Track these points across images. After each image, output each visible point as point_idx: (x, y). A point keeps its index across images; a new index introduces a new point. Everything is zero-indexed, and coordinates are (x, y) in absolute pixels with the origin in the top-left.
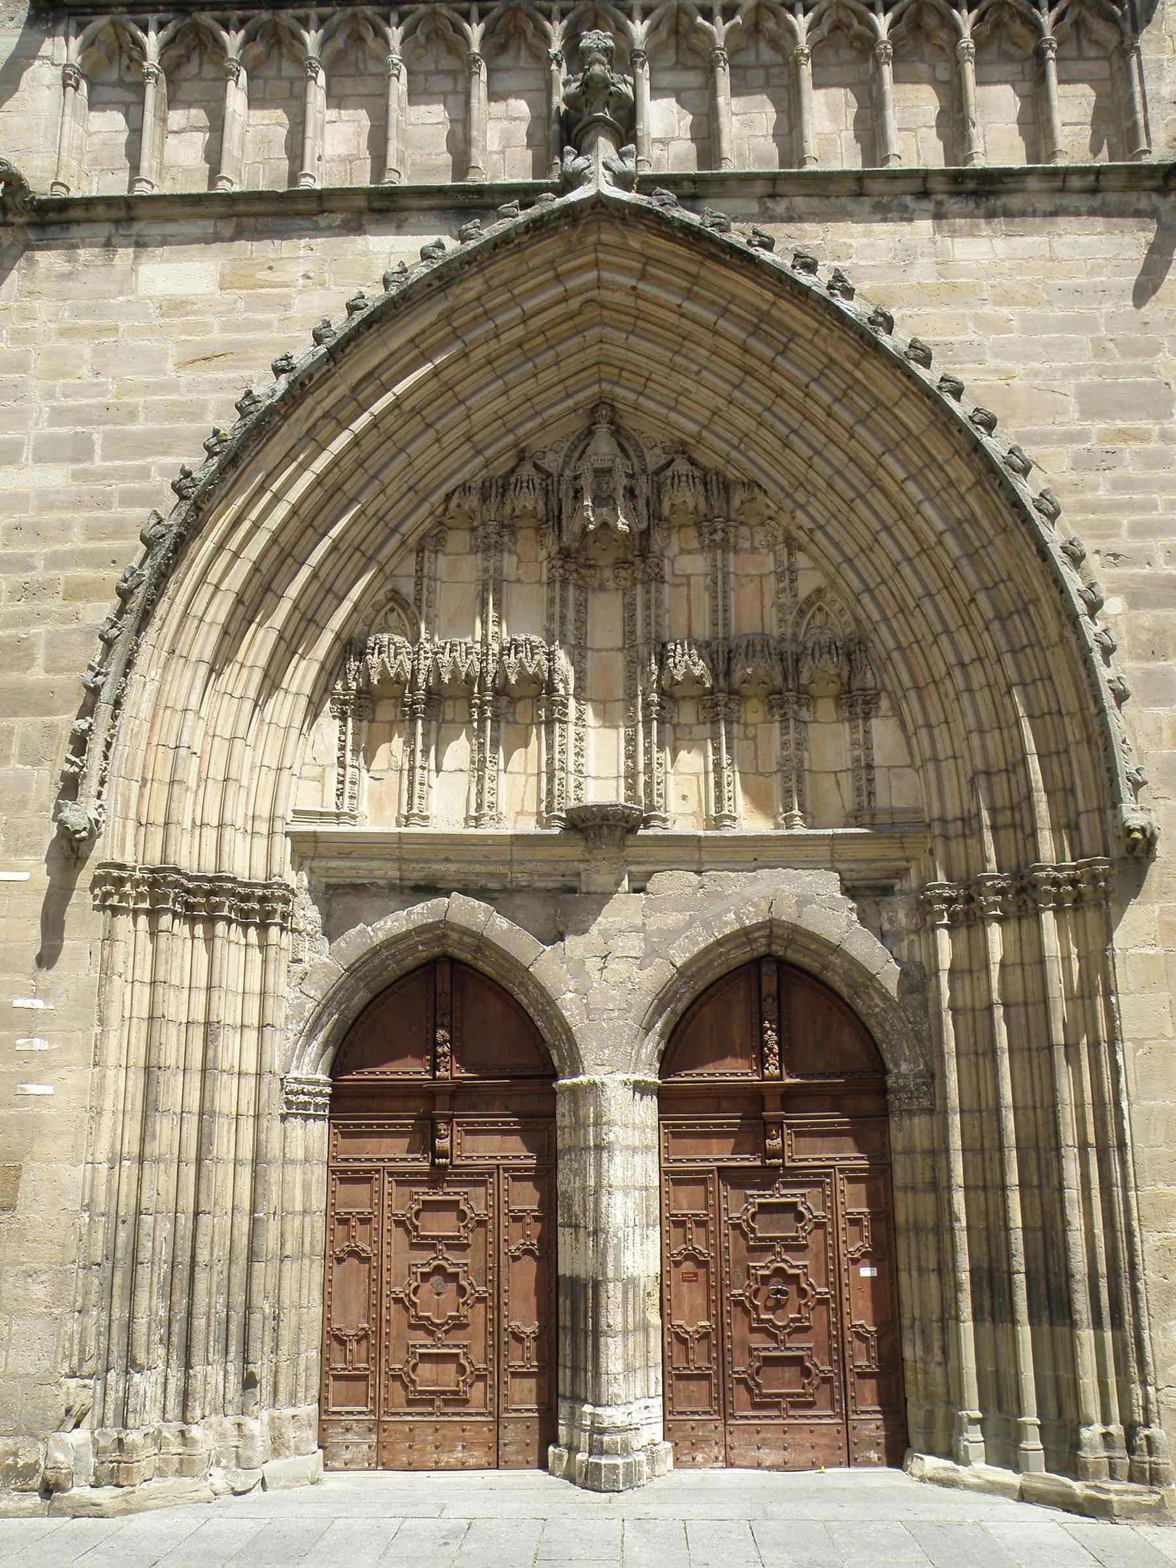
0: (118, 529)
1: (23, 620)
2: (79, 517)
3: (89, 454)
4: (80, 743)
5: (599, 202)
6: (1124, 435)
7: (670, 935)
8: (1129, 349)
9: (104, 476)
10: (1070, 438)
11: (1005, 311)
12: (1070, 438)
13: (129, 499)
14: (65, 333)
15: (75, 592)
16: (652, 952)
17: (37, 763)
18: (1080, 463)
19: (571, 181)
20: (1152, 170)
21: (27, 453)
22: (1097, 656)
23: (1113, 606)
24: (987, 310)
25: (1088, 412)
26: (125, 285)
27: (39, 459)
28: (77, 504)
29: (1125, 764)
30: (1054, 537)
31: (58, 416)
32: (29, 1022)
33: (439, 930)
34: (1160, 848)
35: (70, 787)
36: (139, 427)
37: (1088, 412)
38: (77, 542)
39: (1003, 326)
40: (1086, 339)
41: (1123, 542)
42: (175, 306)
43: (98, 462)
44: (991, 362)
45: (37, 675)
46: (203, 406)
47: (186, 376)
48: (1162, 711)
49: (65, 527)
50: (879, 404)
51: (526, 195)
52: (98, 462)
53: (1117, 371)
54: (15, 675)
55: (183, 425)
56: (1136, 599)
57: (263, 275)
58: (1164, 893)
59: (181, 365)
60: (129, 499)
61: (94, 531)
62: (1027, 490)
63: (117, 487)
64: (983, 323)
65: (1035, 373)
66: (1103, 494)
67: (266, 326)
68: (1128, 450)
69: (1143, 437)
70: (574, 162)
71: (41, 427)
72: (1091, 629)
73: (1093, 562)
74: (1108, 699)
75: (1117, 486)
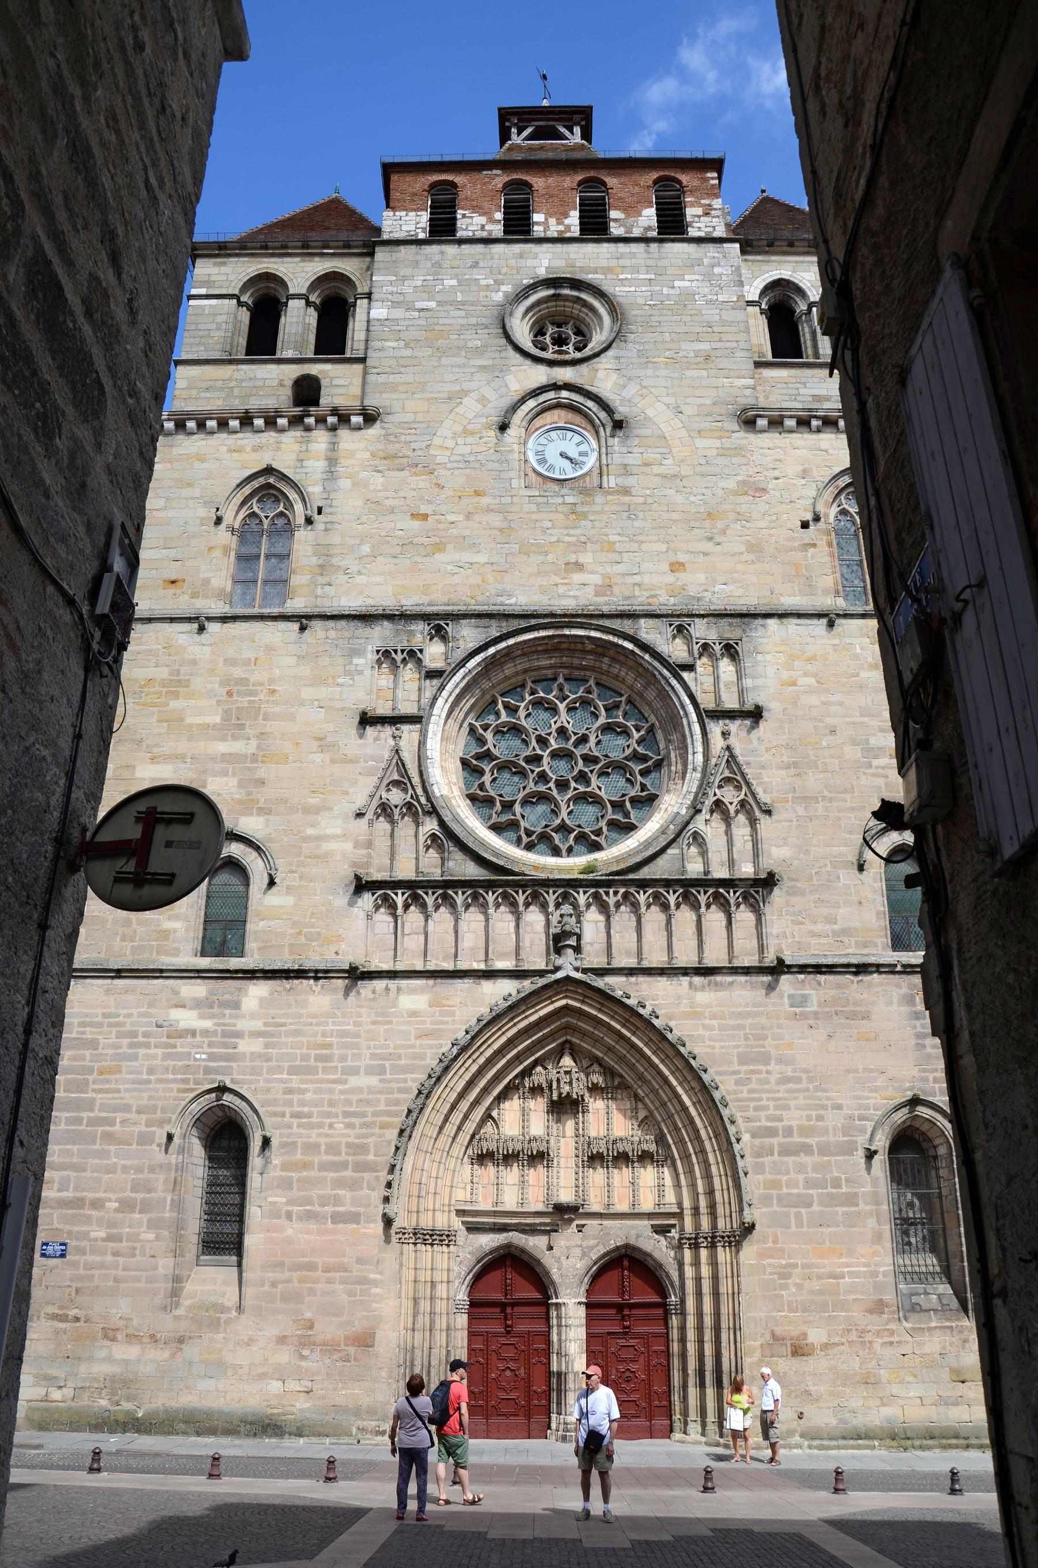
0: (397, 1102)
1: (365, 1136)
2: (383, 1097)
3: (385, 1073)
4: (389, 1185)
5: (568, 979)
6: (753, 1072)
7: (592, 1248)
8: (756, 1037)
9: (390, 1081)
10: (734, 1073)
11: (714, 1023)
12: (734, 1073)
13: (401, 1091)
14: (374, 1023)
15: (383, 1126)
16: (584, 1255)
17: (373, 1190)
18: (738, 1083)
19: (557, 969)
20: (768, 968)
21: (362, 1071)
22: (738, 1158)
23: (746, 1137)
24: (707, 1022)
25: (740, 1063)
26: (394, 1004)
27: (366, 1074)
28: (381, 1092)
29: (746, 1198)
30: (725, 1113)
31: (373, 1056)
32: (375, 1283)
33: (509, 1246)
34: (757, 1227)
35: (386, 1200)
36: (403, 1062)
37: (740, 1063)
38: (382, 1107)
39: (710, 1028)
40: (742, 1033)
41: (751, 1113)
42: (413, 1014)
43: (388, 1076)
44: (708, 1043)
45: (371, 1157)
46: (425, 1054)
47: (418, 1042)
48: (760, 1177)
49: (378, 1101)
50: (667, 1056)
51: (541, 973)
52: (388, 1076)
53: (752, 1046)
54: (362, 1157)
55: (418, 1062)
56: (754, 1136)
57: (445, 1002)
58: (758, 1241)
59: (417, 1038)
60: (401, 1091)
61: (389, 1103)
62: (717, 1095)
63: (395, 1085)
64: (705, 1027)
65: (723, 1047)
66: (745, 1095)
67: (447, 1023)
68: (754, 1077)
69: (759, 1072)
70: (559, 961)
71: (365, 1062)
72: (736, 1147)
73: (740, 1121)
74: (741, 1174)
75: (750, 1091)
